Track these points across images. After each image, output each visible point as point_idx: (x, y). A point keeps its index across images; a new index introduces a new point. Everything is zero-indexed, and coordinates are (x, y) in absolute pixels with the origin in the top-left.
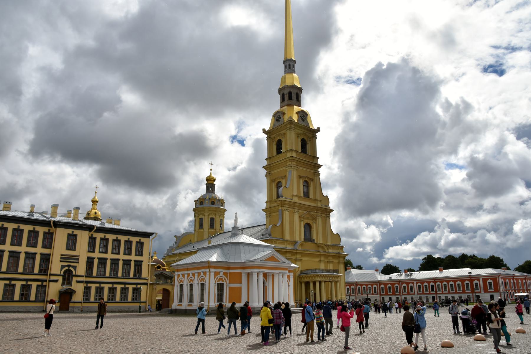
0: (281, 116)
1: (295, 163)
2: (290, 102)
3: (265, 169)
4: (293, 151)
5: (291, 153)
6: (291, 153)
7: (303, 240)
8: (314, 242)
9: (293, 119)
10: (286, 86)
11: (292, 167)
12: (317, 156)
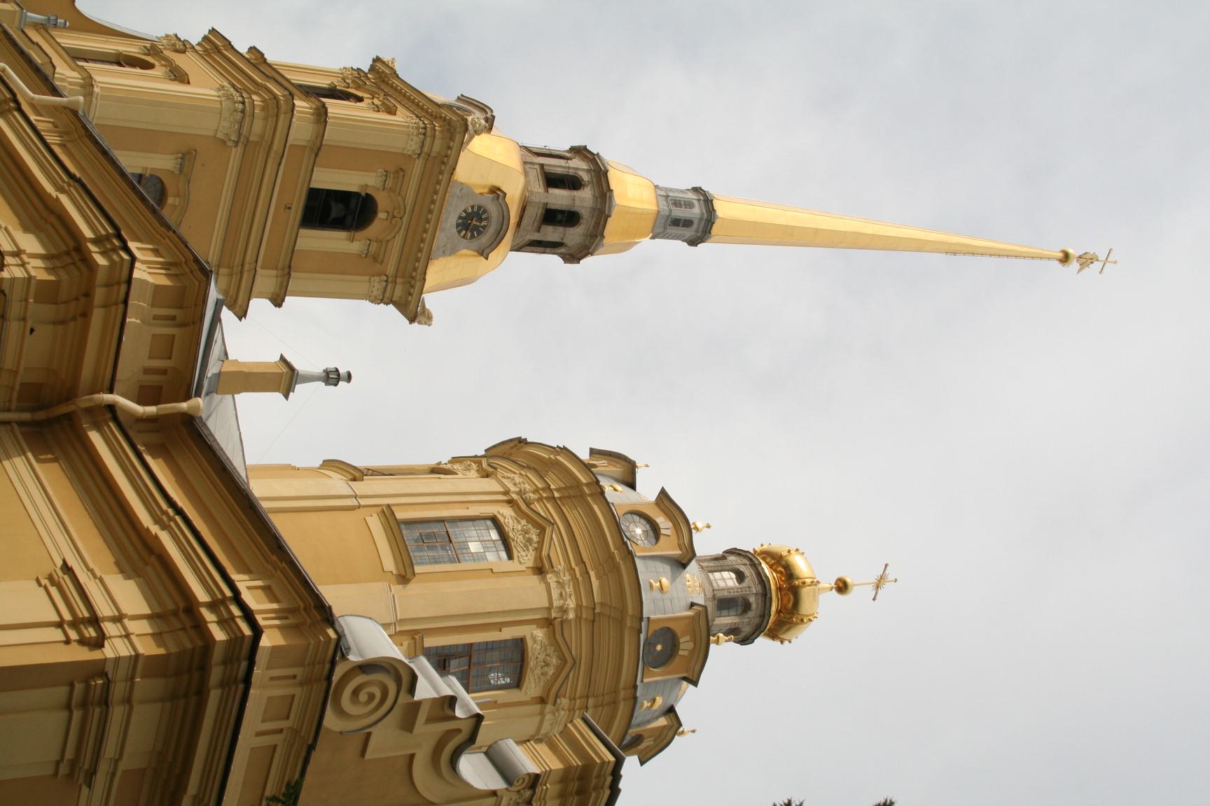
3: (205, 38)
11: (241, 106)
12: (289, 300)
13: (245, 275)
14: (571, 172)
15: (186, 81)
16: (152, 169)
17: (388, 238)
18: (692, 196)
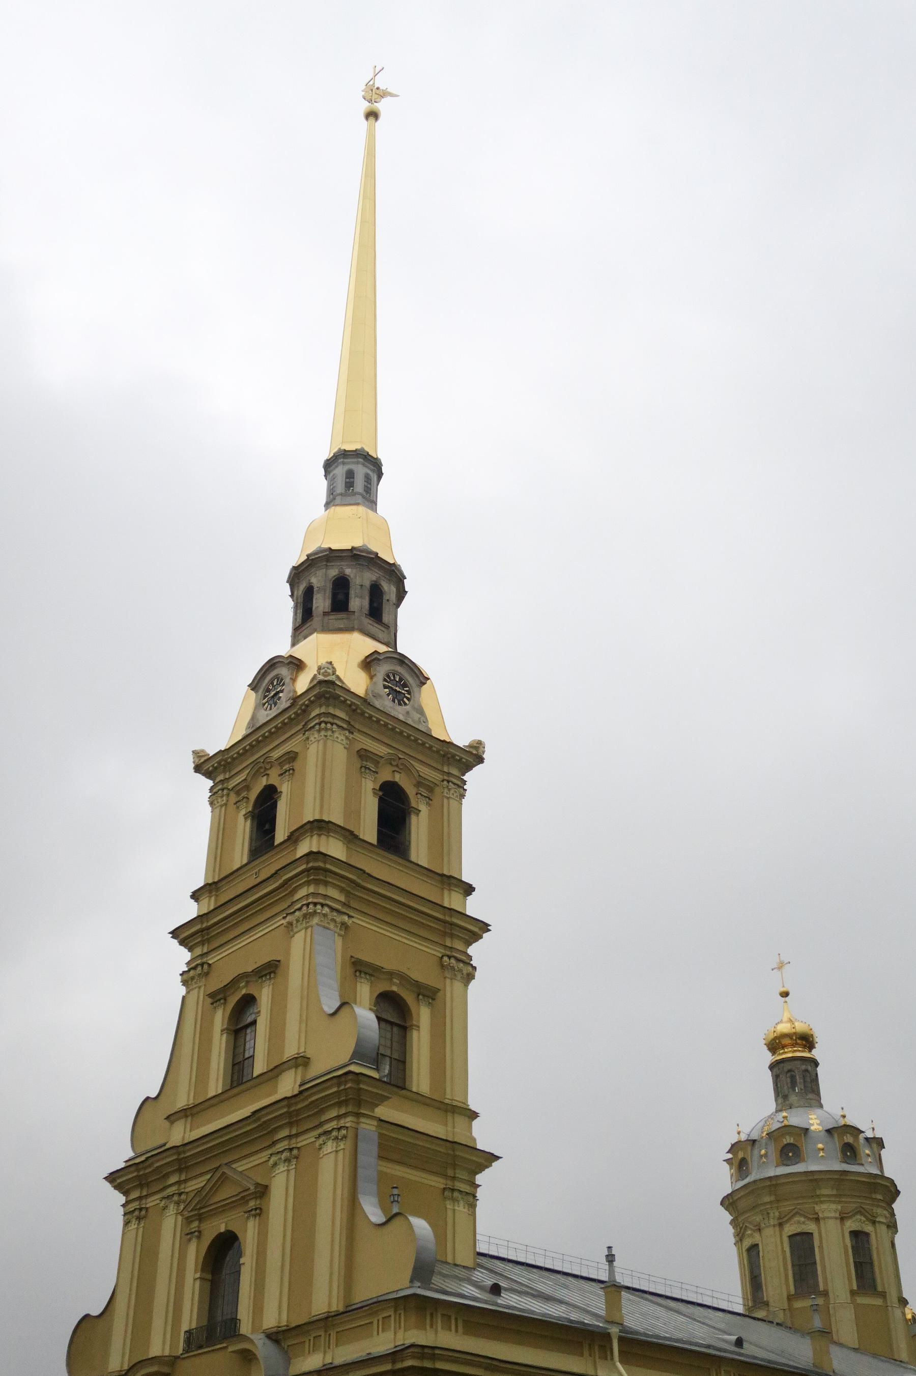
0: (287, 680)
1: (333, 893)
2: (336, 619)
4: (329, 831)
5: (315, 837)
6: (315, 837)
9: (338, 678)
10: (321, 550)
14: (329, 586)
15: (277, 963)
17: (416, 775)
18: (340, 471)
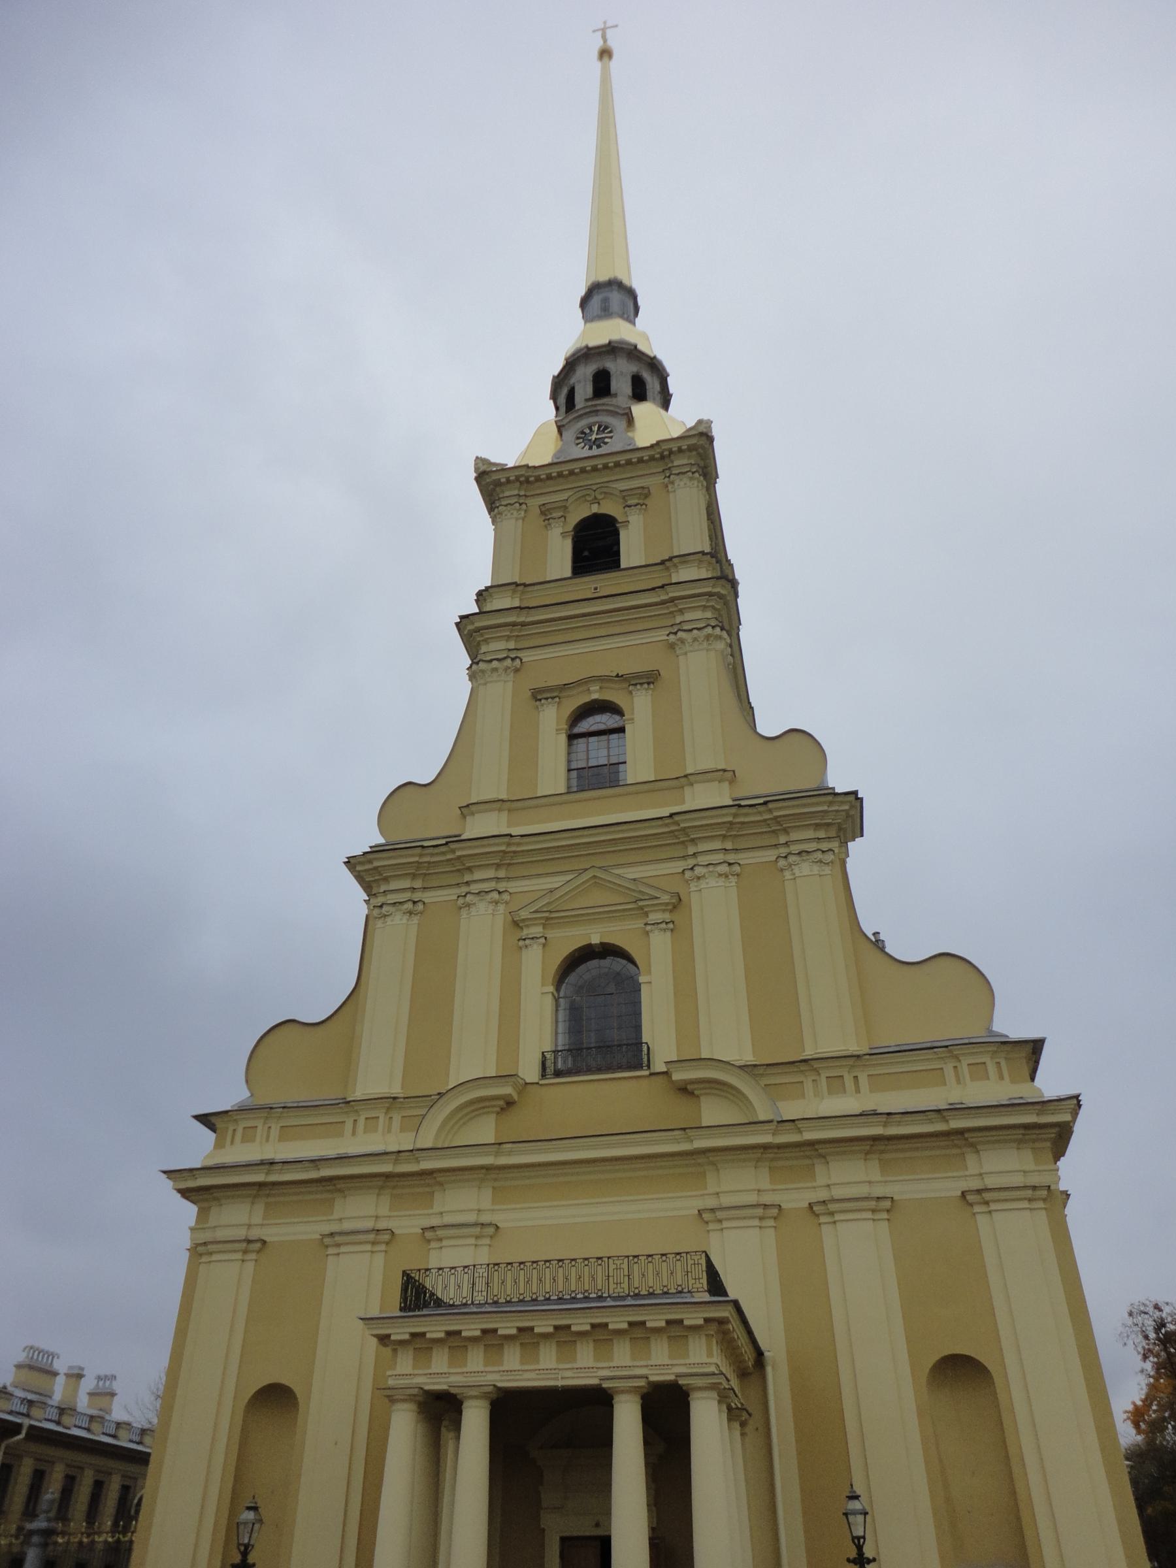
7: (529, 1072)
8: (649, 1067)
13: (671, 595)
16: (558, 723)
